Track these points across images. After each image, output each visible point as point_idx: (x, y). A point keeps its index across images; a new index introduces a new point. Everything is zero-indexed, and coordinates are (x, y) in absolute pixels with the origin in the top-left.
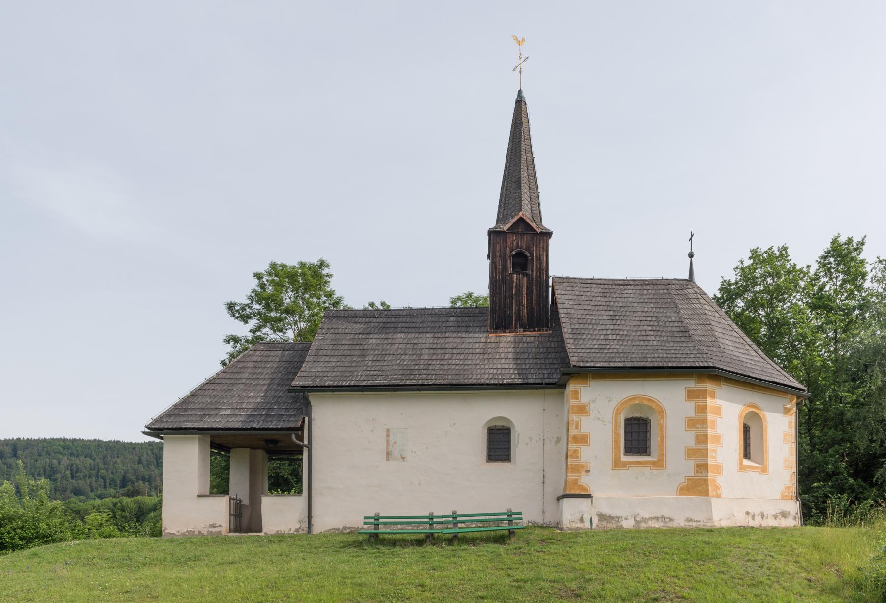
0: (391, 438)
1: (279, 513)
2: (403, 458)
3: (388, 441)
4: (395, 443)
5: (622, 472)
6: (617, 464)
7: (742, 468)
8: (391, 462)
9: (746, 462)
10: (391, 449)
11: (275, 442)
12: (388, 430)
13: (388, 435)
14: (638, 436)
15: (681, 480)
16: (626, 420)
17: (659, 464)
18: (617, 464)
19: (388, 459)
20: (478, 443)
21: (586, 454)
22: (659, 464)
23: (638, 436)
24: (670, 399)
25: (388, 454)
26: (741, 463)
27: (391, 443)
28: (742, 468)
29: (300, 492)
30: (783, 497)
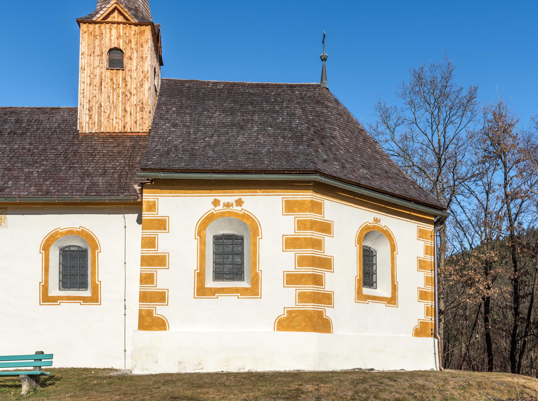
9: (366, 291)
15: (280, 312)
17: (254, 291)
22: (254, 291)
24: (269, 213)
26: (359, 293)
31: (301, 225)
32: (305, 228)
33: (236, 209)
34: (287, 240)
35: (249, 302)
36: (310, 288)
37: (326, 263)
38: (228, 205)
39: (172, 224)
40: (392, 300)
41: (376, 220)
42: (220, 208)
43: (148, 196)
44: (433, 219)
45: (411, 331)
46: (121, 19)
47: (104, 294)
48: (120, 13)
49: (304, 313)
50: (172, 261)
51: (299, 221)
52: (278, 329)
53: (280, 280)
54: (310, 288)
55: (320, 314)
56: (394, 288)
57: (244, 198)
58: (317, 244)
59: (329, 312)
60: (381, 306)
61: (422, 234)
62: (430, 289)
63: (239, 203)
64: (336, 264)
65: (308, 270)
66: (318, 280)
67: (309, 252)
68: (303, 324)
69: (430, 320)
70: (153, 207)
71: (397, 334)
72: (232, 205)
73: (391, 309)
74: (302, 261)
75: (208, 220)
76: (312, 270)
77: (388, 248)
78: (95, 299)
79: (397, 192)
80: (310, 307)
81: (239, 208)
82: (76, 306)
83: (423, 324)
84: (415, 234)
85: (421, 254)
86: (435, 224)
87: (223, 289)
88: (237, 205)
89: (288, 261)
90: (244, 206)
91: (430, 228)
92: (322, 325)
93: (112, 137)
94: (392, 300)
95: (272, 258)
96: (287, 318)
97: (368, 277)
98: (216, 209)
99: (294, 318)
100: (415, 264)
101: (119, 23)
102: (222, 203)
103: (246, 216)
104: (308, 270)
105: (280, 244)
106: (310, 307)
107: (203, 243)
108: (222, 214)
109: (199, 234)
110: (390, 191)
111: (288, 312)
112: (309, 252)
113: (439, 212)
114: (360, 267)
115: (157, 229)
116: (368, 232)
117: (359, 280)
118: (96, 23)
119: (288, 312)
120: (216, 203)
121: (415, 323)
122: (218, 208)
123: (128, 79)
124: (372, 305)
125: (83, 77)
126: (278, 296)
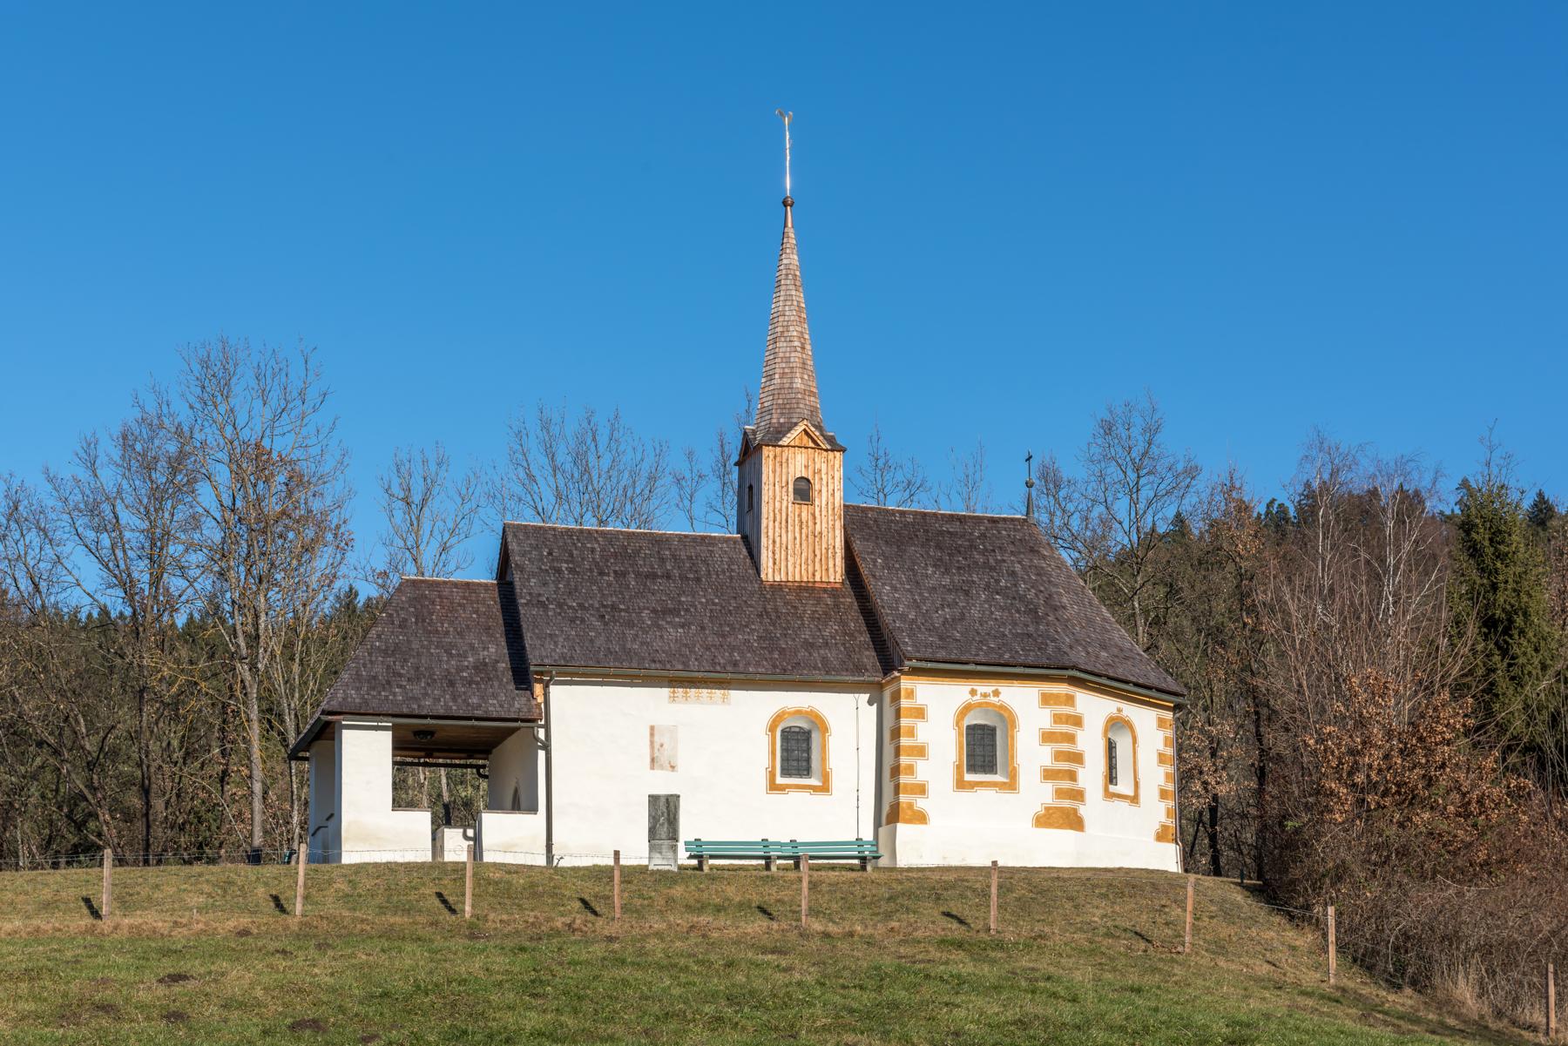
0: (656, 738)
1: (509, 837)
3: (652, 743)
6: (961, 785)
7: (1109, 795)
8: (658, 772)
9: (1112, 788)
10: (657, 754)
11: (432, 733)
12: (652, 728)
13: (652, 735)
14: (983, 749)
17: (1011, 785)
19: (652, 768)
20: (760, 752)
21: (924, 771)
22: (1011, 785)
23: (983, 749)
24: (1025, 704)
25: (653, 760)
26: (1106, 790)
27: (657, 746)
28: (1109, 795)
29: (533, 809)
30: (1161, 837)
31: (1058, 719)
32: (1061, 722)
33: (993, 699)
35: (1007, 797)
36: (1066, 784)
37: (1077, 758)
38: (985, 695)
39: (931, 712)
40: (1134, 799)
43: (906, 683)
45: (1153, 835)
47: (835, 782)
49: (1061, 809)
50: (931, 751)
53: (1038, 775)
54: (1066, 784)
58: (1071, 738)
59: (1083, 811)
60: (1124, 805)
61: (1161, 723)
62: (1171, 787)
63: (996, 693)
64: (1087, 758)
65: (1065, 766)
66: (1072, 776)
67: (1065, 747)
69: (1171, 823)
70: (911, 694)
73: (1134, 809)
74: (1058, 756)
75: (966, 709)
76: (1065, 769)
77: (1130, 740)
78: (825, 788)
80: (1066, 803)
82: (805, 796)
83: (1164, 827)
84: (1154, 723)
89: (1044, 756)
91: (1169, 715)
92: (1074, 822)
93: (806, 589)
94: (1134, 799)
95: (1030, 752)
103: (1003, 707)
104: (1065, 766)
105: (1036, 738)
106: (1066, 803)
108: (979, 705)
111: (1047, 809)
112: (1065, 747)
114: (960, 743)
116: (1117, 723)
119: (1047, 809)
120: (973, 692)
126: (1036, 793)
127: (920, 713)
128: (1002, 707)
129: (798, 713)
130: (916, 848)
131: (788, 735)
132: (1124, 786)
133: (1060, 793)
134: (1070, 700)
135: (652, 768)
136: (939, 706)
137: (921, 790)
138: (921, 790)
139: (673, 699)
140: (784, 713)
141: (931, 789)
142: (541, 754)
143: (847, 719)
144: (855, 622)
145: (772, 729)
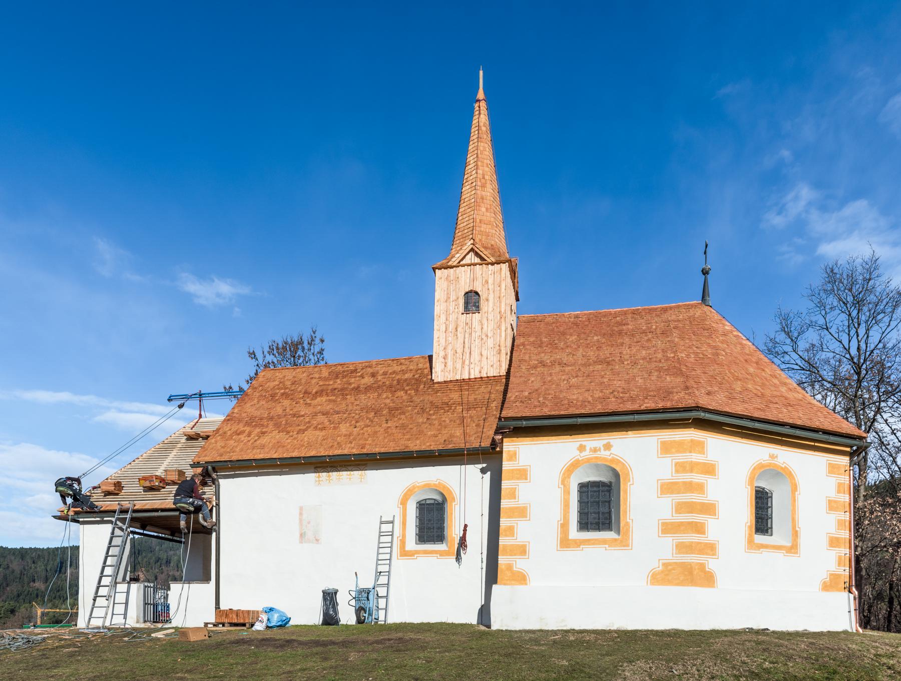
2: (317, 540)
3: (301, 520)
4: (309, 523)
5: (570, 554)
6: (565, 543)
9: (760, 539)
12: (301, 508)
13: (301, 514)
14: (599, 506)
16: (584, 488)
17: (624, 544)
18: (565, 543)
19: (301, 542)
22: (624, 544)
23: (599, 506)
24: (641, 457)
25: (301, 535)
26: (750, 541)
29: (207, 579)
30: (828, 586)
33: (604, 454)
34: (662, 485)
38: (595, 450)
41: (772, 457)
42: (587, 454)
44: (848, 449)
46: (477, 260)
48: (477, 254)
51: (676, 464)
52: (652, 584)
55: (702, 566)
56: (795, 534)
57: (612, 442)
59: (712, 564)
60: (779, 556)
63: (608, 447)
64: (722, 509)
68: (681, 578)
70: (513, 456)
71: (802, 588)
72: (600, 450)
73: (792, 559)
75: (574, 466)
76: (690, 518)
79: (799, 423)
81: (608, 453)
85: (832, 493)
86: (851, 455)
87: (589, 540)
88: (605, 450)
89: (665, 508)
90: (613, 450)
91: (845, 460)
92: (700, 577)
94: (793, 549)
96: (662, 572)
97: (763, 523)
98: (582, 455)
99: (670, 571)
100: (824, 505)
101: (475, 265)
102: (588, 449)
107: (567, 492)
108: (588, 460)
109: (563, 483)
110: (791, 421)
111: (664, 564)
113: (857, 442)
115: (518, 479)
117: (750, 527)
118: (452, 267)
119: (664, 564)
120: (582, 448)
121: (823, 576)
122: (584, 454)
123: (485, 321)
124: (766, 554)
125: (439, 325)
127: (523, 474)
128: (613, 460)
129: (428, 487)
130: (514, 612)
131: (423, 507)
132: (779, 535)
133: (682, 548)
134: (699, 447)
135: (301, 542)
136: (545, 469)
137: (522, 550)
138: (522, 550)
139: (319, 482)
140: (414, 487)
141: (532, 549)
142: (214, 534)
143: (466, 486)
144: (505, 406)
145: (404, 502)
